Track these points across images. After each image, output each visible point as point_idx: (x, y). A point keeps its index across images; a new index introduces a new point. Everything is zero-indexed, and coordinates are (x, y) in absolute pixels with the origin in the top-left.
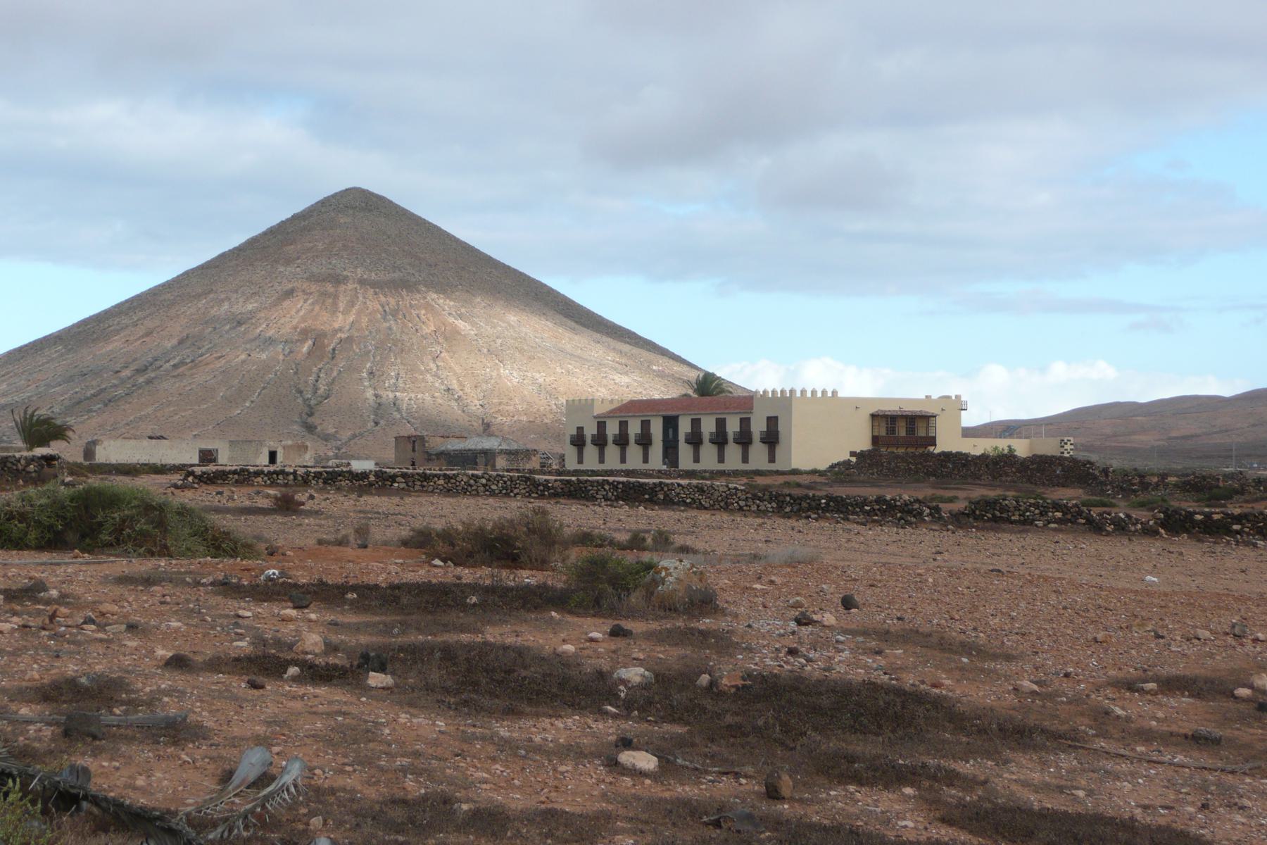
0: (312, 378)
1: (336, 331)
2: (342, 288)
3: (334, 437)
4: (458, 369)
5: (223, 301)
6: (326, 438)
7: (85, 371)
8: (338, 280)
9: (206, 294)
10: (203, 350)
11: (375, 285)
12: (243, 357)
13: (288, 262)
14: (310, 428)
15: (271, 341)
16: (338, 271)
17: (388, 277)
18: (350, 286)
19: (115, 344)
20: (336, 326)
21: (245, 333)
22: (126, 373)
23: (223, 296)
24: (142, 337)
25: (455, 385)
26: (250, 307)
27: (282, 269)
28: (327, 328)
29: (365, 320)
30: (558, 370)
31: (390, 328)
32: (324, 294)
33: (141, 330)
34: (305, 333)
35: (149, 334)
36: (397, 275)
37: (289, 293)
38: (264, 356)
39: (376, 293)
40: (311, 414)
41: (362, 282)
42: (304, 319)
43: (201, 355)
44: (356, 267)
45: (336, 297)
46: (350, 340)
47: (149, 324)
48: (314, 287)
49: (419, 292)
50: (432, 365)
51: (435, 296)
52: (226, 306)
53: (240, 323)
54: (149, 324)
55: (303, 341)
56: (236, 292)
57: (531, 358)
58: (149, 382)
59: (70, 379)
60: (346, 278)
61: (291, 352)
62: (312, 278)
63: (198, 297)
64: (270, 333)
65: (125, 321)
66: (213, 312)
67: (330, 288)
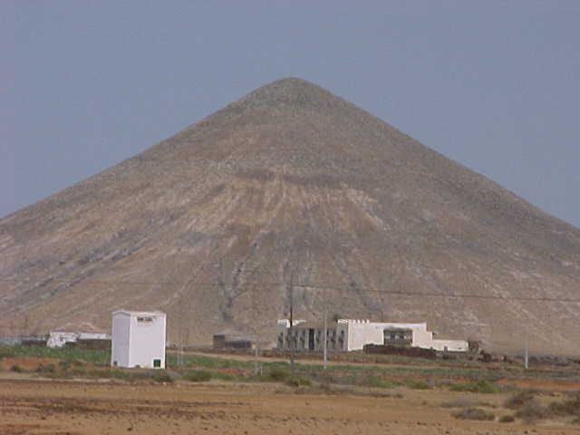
0: (234, 272)
1: (259, 227)
2: (269, 184)
4: (366, 265)
5: (158, 196)
7: (33, 262)
8: (265, 176)
9: (144, 187)
10: (138, 245)
11: (304, 182)
12: (174, 251)
13: (221, 157)
15: (198, 238)
16: (266, 167)
18: (276, 182)
20: (260, 221)
21: (179, 226)
23: (159, 191)
24: (84, 230)
27: (212, 164)
28: (251, 224)
30: (460, 266)
31: (308, 225)
32: (251, 191)
34: (232, 229)
35: (91, 226)
37: (220, 189)
38: (192, 251)
39: (299, 190)
40: (229, 306)
41: (287, 178)
42: (231, 215)
43: (137, 249)
44: (282, 164)
45: (262, 193)
46: (271, 236)
49: (340, 188)
50: (343, 261)
51: (353, 192)
52: (161, 201)
53: (172, 218)
56: (171, 186)
58: (91, 273)
60: (272, 176)
61: (217, 247)
62: (241, 174)
63: (135, 191)
66: (151, 207)
67: (257, 185)
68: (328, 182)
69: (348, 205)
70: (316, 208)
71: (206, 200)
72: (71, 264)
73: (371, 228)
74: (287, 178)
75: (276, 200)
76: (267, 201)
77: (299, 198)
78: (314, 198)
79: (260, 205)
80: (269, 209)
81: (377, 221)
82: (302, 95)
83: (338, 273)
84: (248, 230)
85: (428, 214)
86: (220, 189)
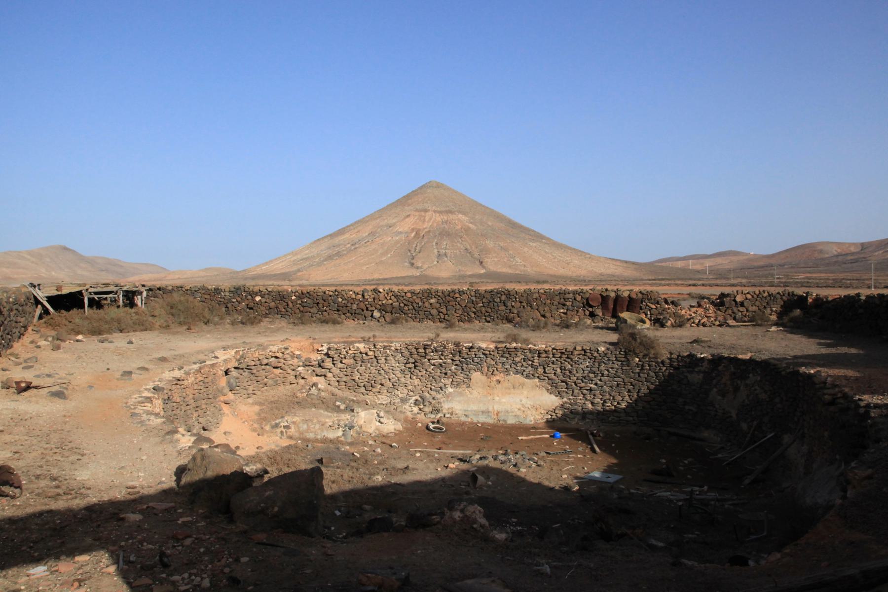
3: (421, 268)
6: (418, 268)
8: (426, 211)
11: (440, 212)
13: (409, 205)
14: (413, 264)
15: (401, 233)
19: (347, 236)
25: (468, 247)
29: (435, 225)
32: (421, 216)
34: (413, 230)
37: (408, 216)
41: (435, 211)
46: (429, 231)
47: (359, 228)
48: (417, 214)
59: (329, 248)
62: (417, 210)
63: (377, 219)
67: (423, 214)
68: (451, 212)
69: (459, 220)
73: (469, 228)
74: (435, 211)
75: (430, 219)
76: (427, 219)
77: (439, 218)
78: (446, 218)
79: (424, 221)
80: (428, 222)
81: (471, 225)
82: (439, 186)
85: (490, 223)
86: (408, 216)
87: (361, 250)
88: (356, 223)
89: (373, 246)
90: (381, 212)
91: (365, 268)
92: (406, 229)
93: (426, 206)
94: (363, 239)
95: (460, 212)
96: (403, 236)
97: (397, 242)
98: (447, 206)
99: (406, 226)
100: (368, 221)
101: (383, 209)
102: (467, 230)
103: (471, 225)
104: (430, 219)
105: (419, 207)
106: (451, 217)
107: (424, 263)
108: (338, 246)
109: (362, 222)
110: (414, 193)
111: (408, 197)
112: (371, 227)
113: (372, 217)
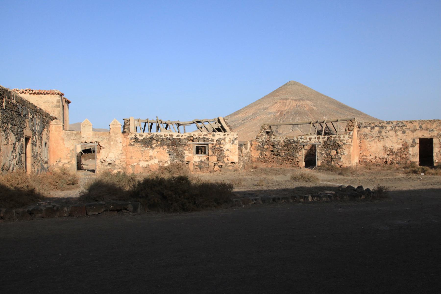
0: (279, 120)
2: (288, 101)
3: (282, 134)
4: (313, 118)
8: (287, 99)
11: (296, 100)
13: (277, 96)
15: (271, 113)
17: (298, 98)
18: (289, 100)
19: (240, 115)
22: (241, 121)
26: (267, 106)
29: (292, 108)
32: (283, 102)
33: (245, 112)
34: (279, 111)
36: (300, 98)
37: (276, 103)
41: (292, 100)
42: (279, 108)
45: (286, 103)
46: (288, 112)
47: (247, 111)
48: (281, 101)
54: (247, 111)
55: (278, 113)
57: (330, 114)
58: (244, 123)
62: (281, 99)
63: (257, 105)
64: (271, 111)
65: (243, 110)
66: (260, 108)
67: (285, 101)
68: (302, 100)
69: (307, 104)
70: (299, 106)
71: (273, 105)
72: (241, 121)
73: (313, 109)
74: (292, 100)
76: (287, 105)
77: (294, 103)
78: (299, 103)
79: (286, 105)
80: (288, 106)
81: (314, 107)
82: (295, 84)
83: (306, 120)
84: (282, 111)
85: (326, 106)
87: (247, 123)
88: (246, 107)
89: (255, 121)
90: (260, 101)
91: (249, 134)
92: (275, 111)
93: (287, 96)
94: (249, 117)
95: (307, 100)
96: (272, 115)
97: (269, 118)
98: (300, 96)
99: (274, 109)
100: (252, 106)
101: (262, 98)
102: (312, 110)
103: (314, 107)
104: (290, 104)
105: (283, 97)
106: (302, 102)
107: (284, 131)
108: (234, 121)
109: (249, 107)
110: (280, 89)
111: (276, 91)
112: (254, 110)
113: (254, 104)
